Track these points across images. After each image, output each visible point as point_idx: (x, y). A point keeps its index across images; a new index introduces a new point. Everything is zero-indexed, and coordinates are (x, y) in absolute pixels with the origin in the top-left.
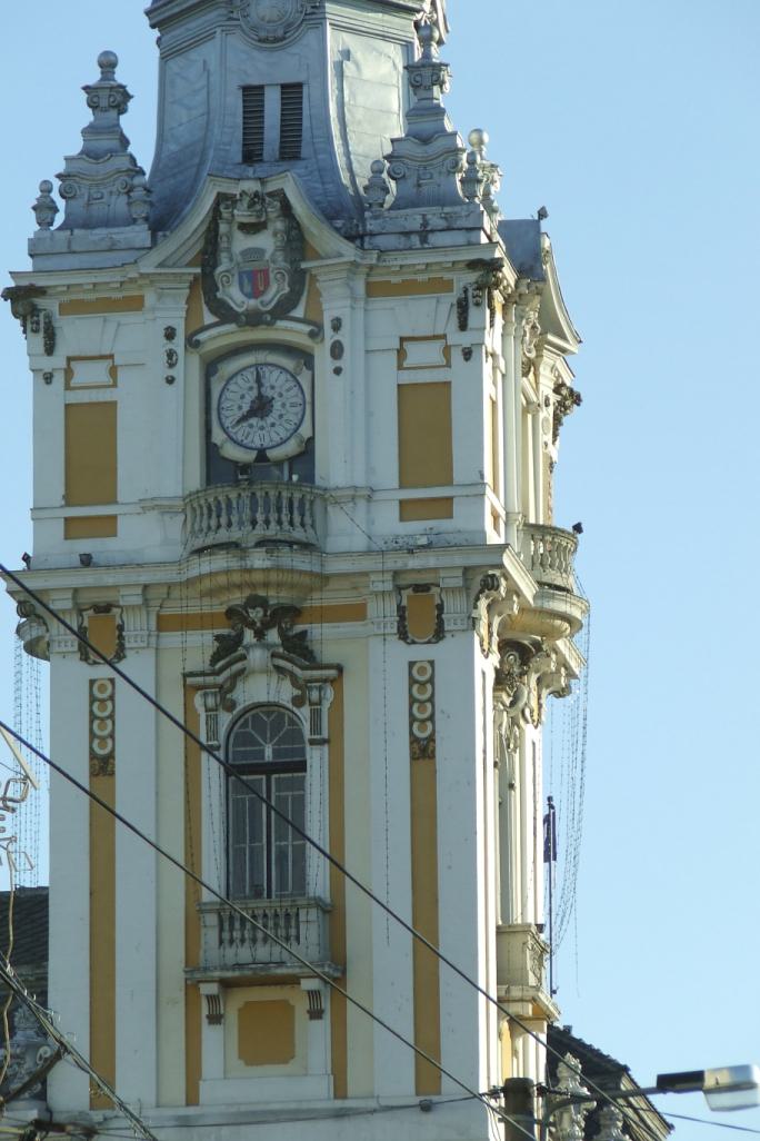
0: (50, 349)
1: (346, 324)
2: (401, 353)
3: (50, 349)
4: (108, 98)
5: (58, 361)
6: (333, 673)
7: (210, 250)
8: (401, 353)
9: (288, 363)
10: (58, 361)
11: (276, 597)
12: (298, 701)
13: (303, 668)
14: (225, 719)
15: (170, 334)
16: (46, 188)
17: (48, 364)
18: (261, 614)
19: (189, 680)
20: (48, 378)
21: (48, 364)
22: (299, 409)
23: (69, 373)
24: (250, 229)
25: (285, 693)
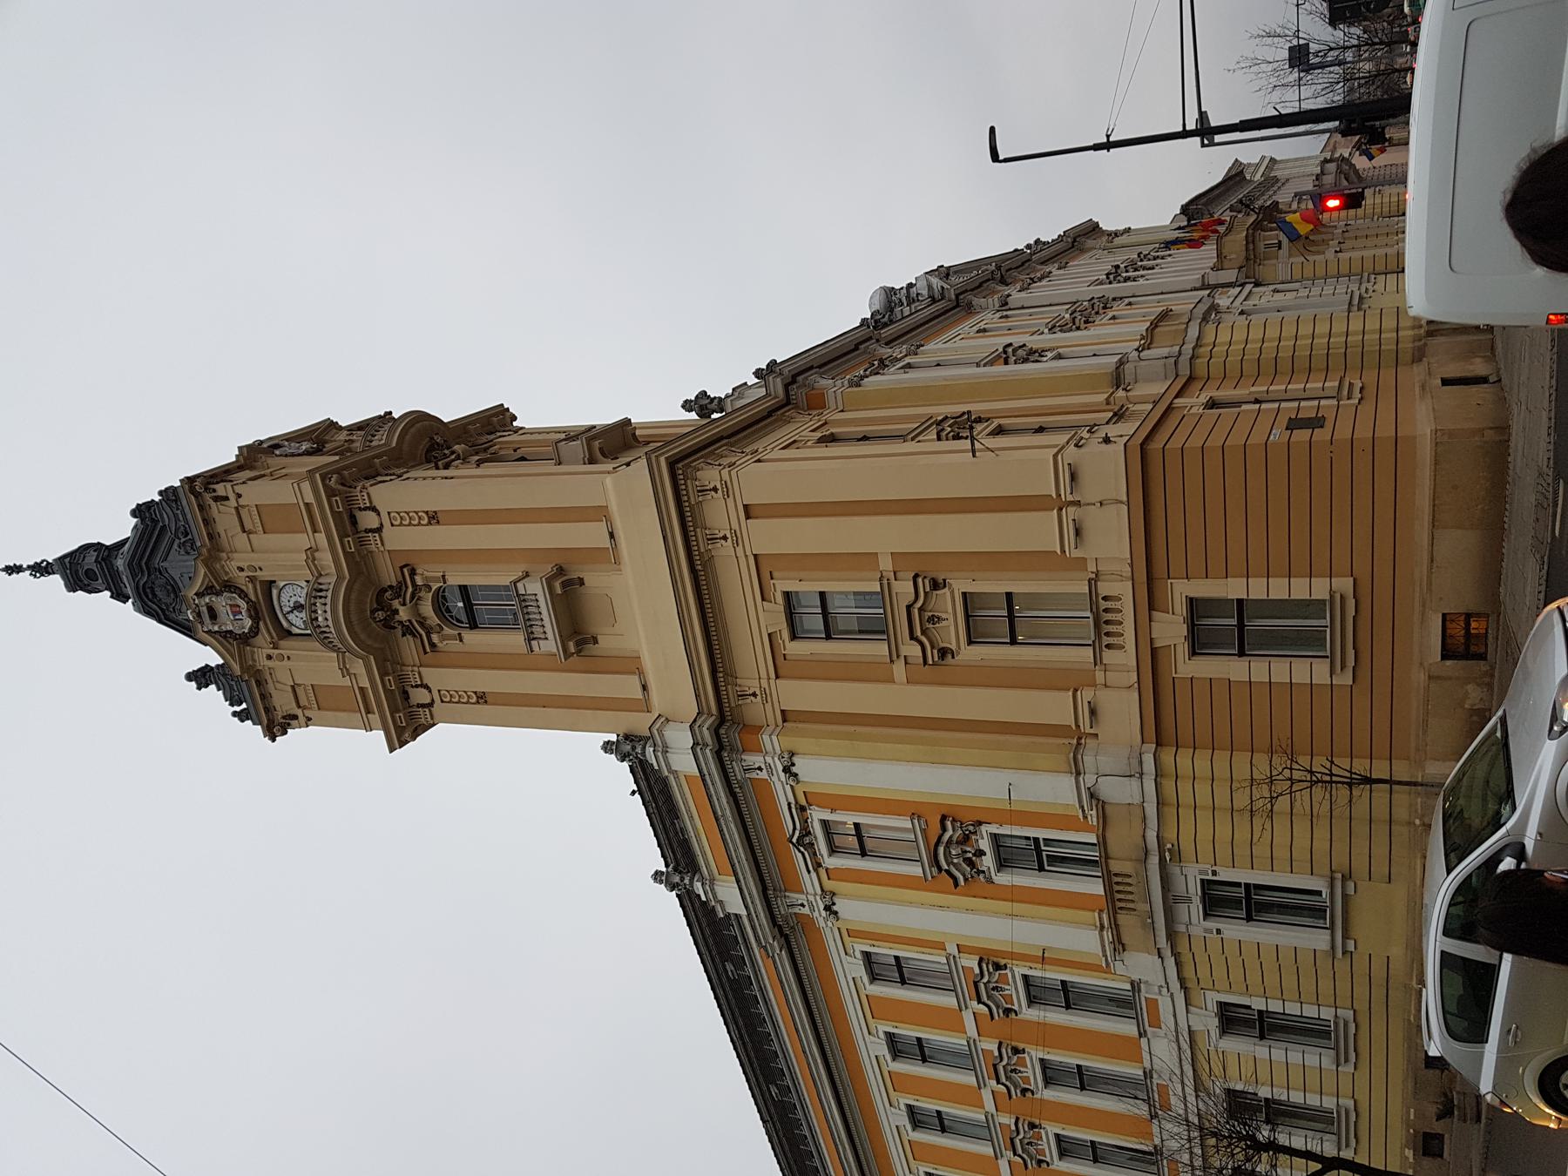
0: (295, 717)
1: (241, 564)
3: (295, 717)
5: (299, 712)
6: (405, 570)
7: (255, 625)
8: (249, 533)
9: (275, 592)
10: (299, 712)
11: (370, 603)
13: (407, 587)
14: (447, 631)
15: (269, 657)
16: (235, 714)
17: (302, 719)
18: (380, 613)
19: (428, 650)
20: (309, 719)
21: (302, 719)
22: (295, 587)
23: (304, 708)
24: (213, 615)
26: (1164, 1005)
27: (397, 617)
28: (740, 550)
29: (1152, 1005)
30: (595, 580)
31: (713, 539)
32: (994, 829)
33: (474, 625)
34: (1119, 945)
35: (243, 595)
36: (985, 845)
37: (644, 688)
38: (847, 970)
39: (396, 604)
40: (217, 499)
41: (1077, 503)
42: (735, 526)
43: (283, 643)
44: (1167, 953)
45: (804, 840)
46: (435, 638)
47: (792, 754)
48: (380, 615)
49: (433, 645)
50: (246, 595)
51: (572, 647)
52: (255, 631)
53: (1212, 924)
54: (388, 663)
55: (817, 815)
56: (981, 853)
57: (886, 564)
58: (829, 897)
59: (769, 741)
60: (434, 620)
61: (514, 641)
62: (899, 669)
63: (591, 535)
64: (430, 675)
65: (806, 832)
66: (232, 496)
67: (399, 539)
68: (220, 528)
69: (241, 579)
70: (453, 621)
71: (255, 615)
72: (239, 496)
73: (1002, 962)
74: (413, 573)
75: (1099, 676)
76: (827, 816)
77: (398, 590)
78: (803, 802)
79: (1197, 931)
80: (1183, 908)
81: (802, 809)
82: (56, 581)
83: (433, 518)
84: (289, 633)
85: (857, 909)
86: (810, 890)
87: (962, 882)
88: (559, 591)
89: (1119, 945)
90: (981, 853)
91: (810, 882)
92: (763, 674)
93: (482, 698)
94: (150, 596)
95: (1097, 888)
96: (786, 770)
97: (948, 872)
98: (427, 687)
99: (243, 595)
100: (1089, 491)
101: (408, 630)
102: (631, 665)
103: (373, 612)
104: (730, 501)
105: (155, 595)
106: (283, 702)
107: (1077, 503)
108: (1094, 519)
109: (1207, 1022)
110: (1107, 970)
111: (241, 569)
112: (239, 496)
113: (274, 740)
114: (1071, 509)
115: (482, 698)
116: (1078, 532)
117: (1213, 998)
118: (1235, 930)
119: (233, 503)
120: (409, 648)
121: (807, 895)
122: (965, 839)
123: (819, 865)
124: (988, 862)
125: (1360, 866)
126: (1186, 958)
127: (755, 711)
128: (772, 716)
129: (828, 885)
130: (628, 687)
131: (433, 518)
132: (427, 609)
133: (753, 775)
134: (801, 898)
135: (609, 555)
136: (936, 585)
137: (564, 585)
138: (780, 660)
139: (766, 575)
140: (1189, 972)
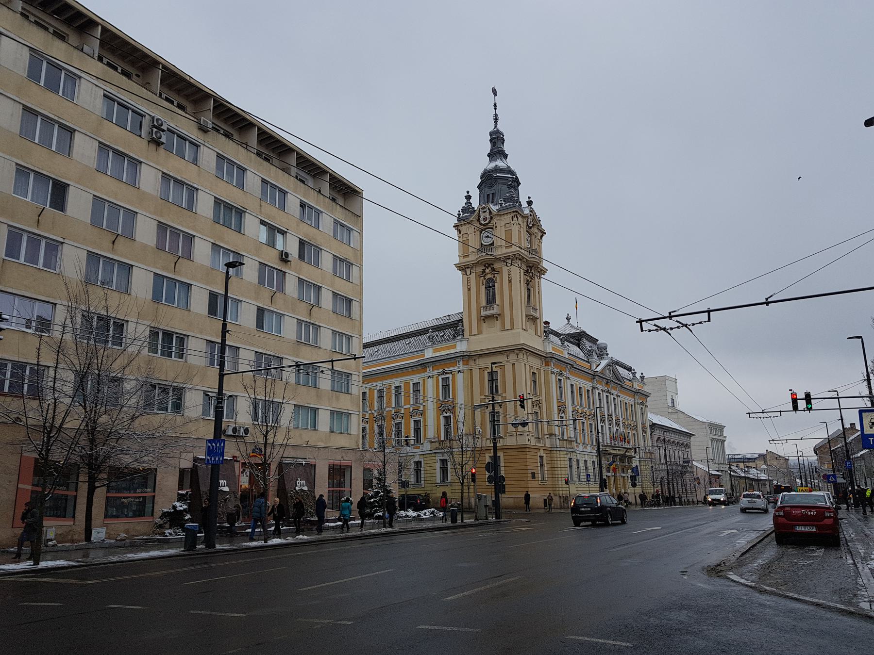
0: (460, 233)
2: (505, 226)
3: (460, 233)
4: (468, 197)
5: (461, 234)
8: (505, 226)
10: (461, 234)
12: (494, 277)
14: (484, 281)
17: (460, 235)
21: (460, 235)
24: (484, 212)
25: (491, 276)
26: (419, 450)
27: (487, 269)
28: (505, 362)
29: (419, 448)
30: (498, 323)
31: (507, 356)
32: (452, 416)
33: (486, 288)
34: (431, 442)
35: (489, 222)
36: (448, 414)
37: (475, 335)
38: (416, 378)
39: (490, 269)
40: (512, 218)
41: (516, 435)
42: (510, 361)
43: (478, 232)
44: (431, 452)
45: (444, 373)
46: (483, 278)
47: (463, 372)
48: (487, 265)
49: (481, 277)
50: (489, 223)
51: (483, 318)
52: (481, 224)
53: (438, 461)
54: (476, 264)
55: (450, 376)
56: (446, 413)
57: (504, 395)
58: (432, 377)
59: (465, 368)
60: (487, 277)
61: (484, 303)
62: (483, 397)
63: (508, 326)
64: (473, 275)
65: (446, 373)
66: (512, 222)
67: (505, 269)
68: (506, 217)
69: (494, 221)
70: (487, 283)
71: (484, 225)
72: (513, 224)
73: (423, 415)
74: (498, 273)
75: (485, 439)
76: (450, 379)
77: (493, 269)
78: (453, 373)
79: (437, 458)
80: (441, 455)
81: (451, 373)
82: (491, 128)
83: (510, 281)
84: (481, 233)
85: (430, 383)
86: (433, 372)
87: (440, 408)
88: (495, 316)
89: (431, 442)
90: (446, 413)
91: (435, 373)
92: (480, 365)
93: (469, 289)
94: (489, 178)
95: (442, 439)
96: (459, 371)
97: (441, 406)
98: (471, 274)
99: (489, 222)
100: (519, 438)
101: (484, 271)
102: (480, 332)
103: (487, 264)
104: (515, 360)
105: (489, 179)
106: (464, 229)
107: (516, 435)
108: (514, 438)
109: (417, 459)
110: (425, 439)
111: (496, 223)
112: (513, 224)
113: (454, 227)
114: (515, 434)
115: (469, 289)
116: (511, 435)
117: (422, 460)
118: (438, 465)
119: (512, 222)
120: (480, 269)
121: (431, 372)
122: (449, 410)
123: (439, 375)
124: (445, 415)
125: (454, 488)
126: (430, 455)
127: (471, 363)
128: (471, 367)
129: (435, 377)
130: (475, 331)
131: (510, 281)
132: (489, 276)
133: (458, 363)
134: (431, 370)
135: (504, 329)
136: (500, 406)
137: (497, 317)
138: (483, 369)
139: (500, 367)
140: (427, 456)
